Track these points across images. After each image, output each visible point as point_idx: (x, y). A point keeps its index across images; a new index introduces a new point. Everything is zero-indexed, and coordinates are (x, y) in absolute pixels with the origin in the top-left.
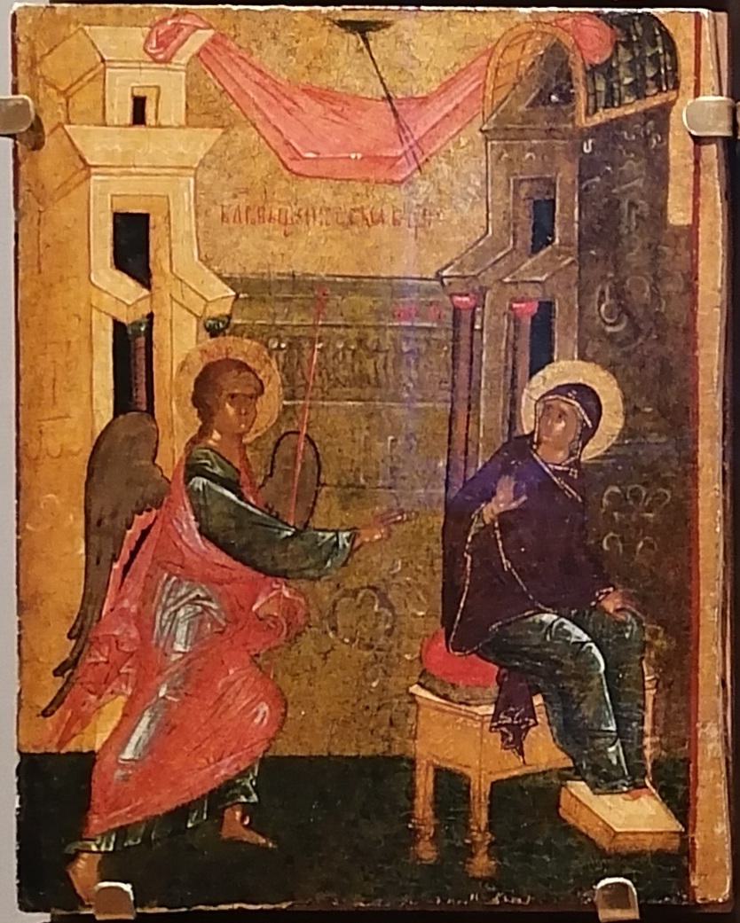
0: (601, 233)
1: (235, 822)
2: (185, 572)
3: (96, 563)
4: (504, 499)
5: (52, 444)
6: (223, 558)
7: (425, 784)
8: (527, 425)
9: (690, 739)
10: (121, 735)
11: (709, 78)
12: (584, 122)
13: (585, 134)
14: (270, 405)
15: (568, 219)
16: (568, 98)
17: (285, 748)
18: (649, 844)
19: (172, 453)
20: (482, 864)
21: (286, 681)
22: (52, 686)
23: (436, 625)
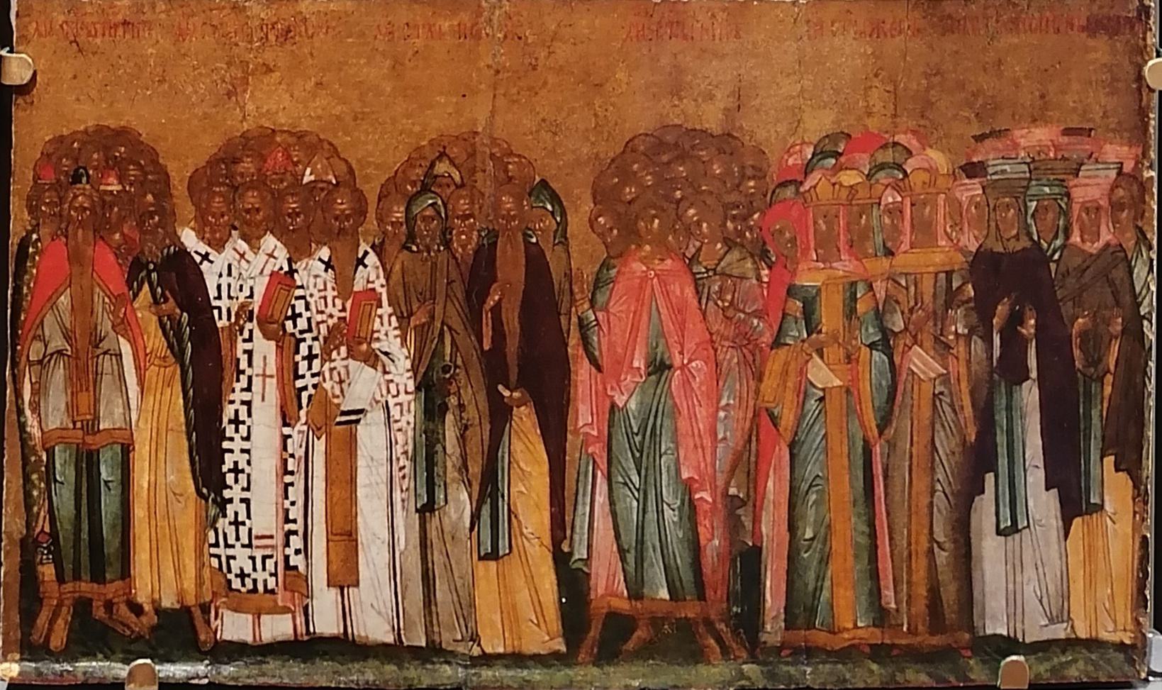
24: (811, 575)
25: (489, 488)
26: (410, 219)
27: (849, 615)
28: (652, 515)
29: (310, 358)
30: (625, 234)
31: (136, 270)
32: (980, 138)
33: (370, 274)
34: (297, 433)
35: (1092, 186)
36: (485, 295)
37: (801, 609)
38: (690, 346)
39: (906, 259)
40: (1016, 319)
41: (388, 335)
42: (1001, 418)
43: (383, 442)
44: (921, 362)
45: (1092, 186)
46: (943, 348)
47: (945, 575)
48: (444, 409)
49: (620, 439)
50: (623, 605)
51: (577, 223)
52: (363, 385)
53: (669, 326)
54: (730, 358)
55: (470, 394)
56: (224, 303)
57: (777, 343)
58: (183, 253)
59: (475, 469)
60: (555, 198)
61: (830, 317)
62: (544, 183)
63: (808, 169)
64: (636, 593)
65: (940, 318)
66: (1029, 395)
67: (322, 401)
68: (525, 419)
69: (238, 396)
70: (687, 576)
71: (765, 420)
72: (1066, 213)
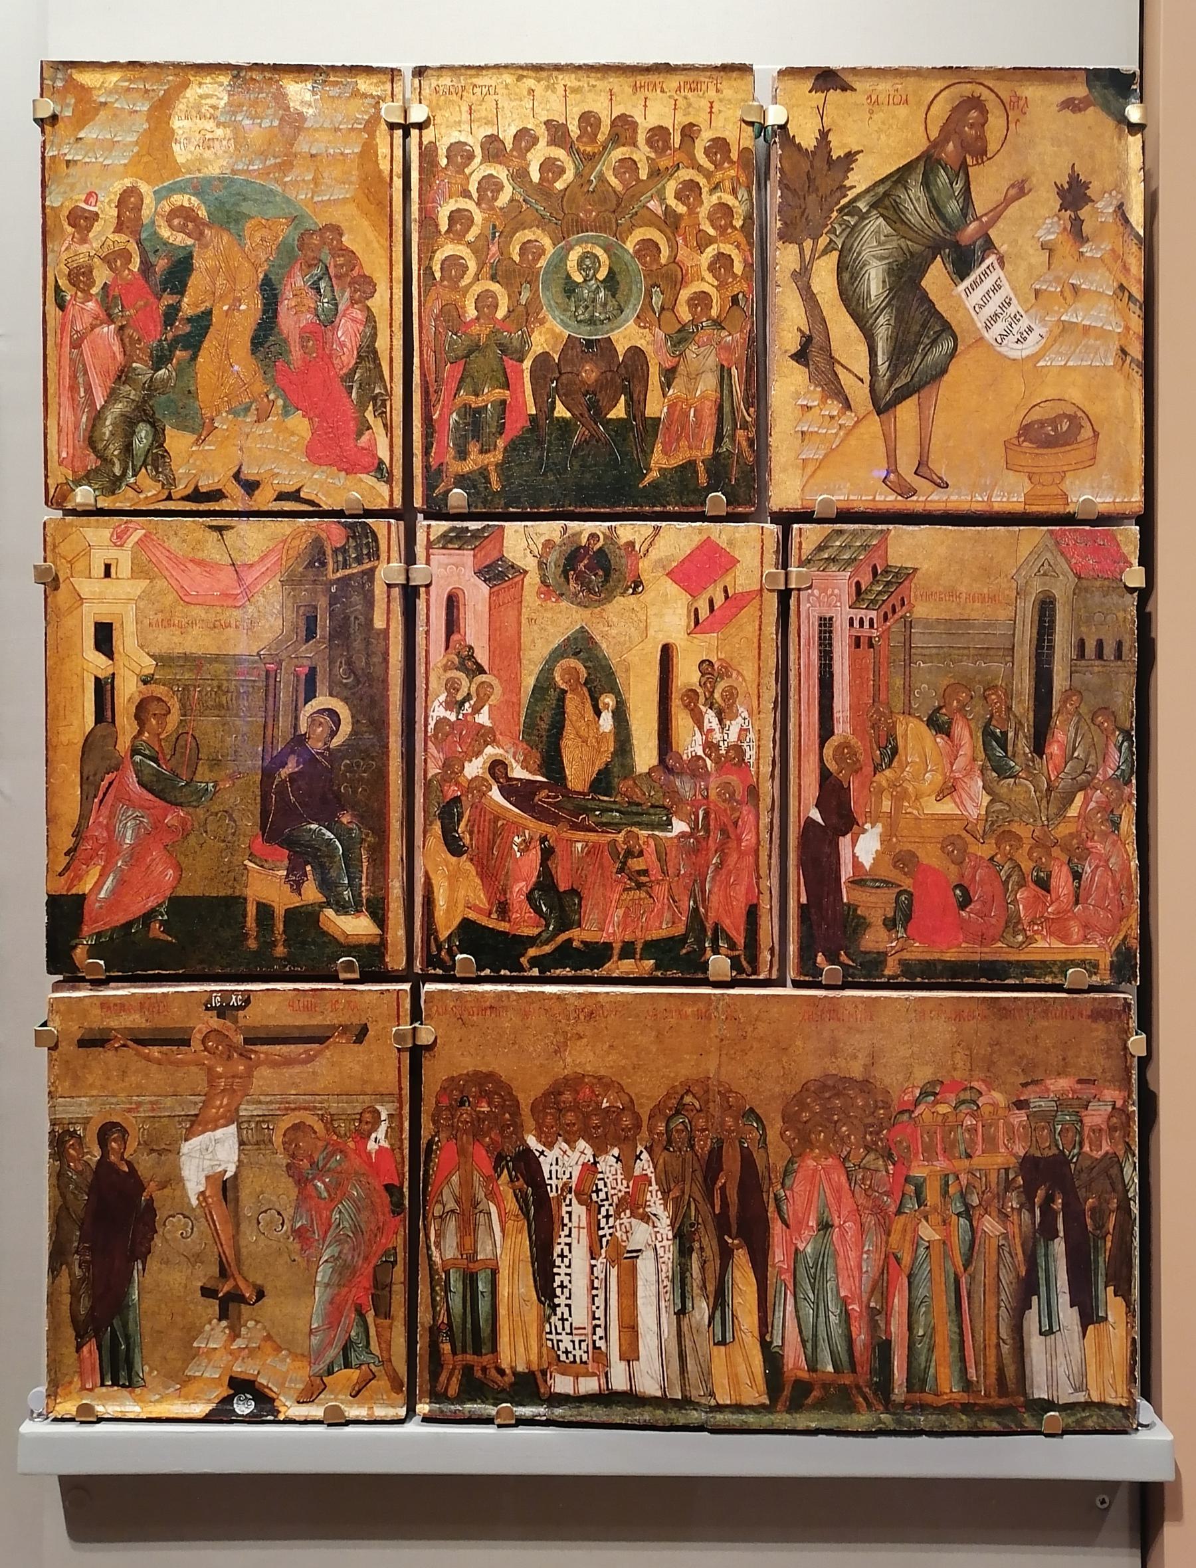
0: (340, 633)
1: (156, 929)
2: (131, 804)
3: (86, 799)
4: (291, 767)
5: (64, 739)
6: (150, 796)
7: (251, 910)
8: (303, 729)
9: (385, 888)
10: (98, 885)
11: (394, 554)
12: (332, 576)
13: (332, 583)
14: (174, 719)
15: (324, 625)
16: (323, 564)
17: (181, 892)
18: (364, 941)
19: (124, 744)
20: (280, 951)
21: (181, 858)
22: (64, 861)
23: (257, 830)
24: (923, 1359)
25: (720, 1300)
26: (668, 1131)
27: (947, 1385)
28: (822, 1319)
29: (607, 1217)
30: (803, 1142)
31: (499, 1161)
32: (1025, 1085)
33: (644, 1165)
34: (600, 1263)
35: (1096, 1116)
36: (715, 1179)
37: (916, 1380)
38: (844, 1213)
39: (979, 1161)
40: (1049, 1199)
41: (655, 1204)
42: (1041, 1261)
43: (653, 1270)
44: (990, 1225)
45: (1096, 1116)
46: (1004, 1217)
47: (1008, 1360)
48: (691, 1250)
49: (801, 1271)
50: (805, 1375)
51: (772, 1135)
52: (640, 1235)
53: (831, 1200)
54: (870, 1220)
55: (707, 1241)
56: (554, 1182)
57: (899, 1212)
58: (528, 1150)
59: (711, 1288)
60: (759, 1119)
61: (932, 1196)
62: (752, 1110)
63: (917, 1103)
64: (813, 1367)
65: (1001, 1197)
66: (1059, 1247)
67: (615, 1244)
68: (741, 1257)
69: (563, 1240)
70: (844, 1357)
71: (892, 1257)
72: (1080, 1133)
